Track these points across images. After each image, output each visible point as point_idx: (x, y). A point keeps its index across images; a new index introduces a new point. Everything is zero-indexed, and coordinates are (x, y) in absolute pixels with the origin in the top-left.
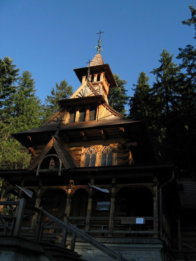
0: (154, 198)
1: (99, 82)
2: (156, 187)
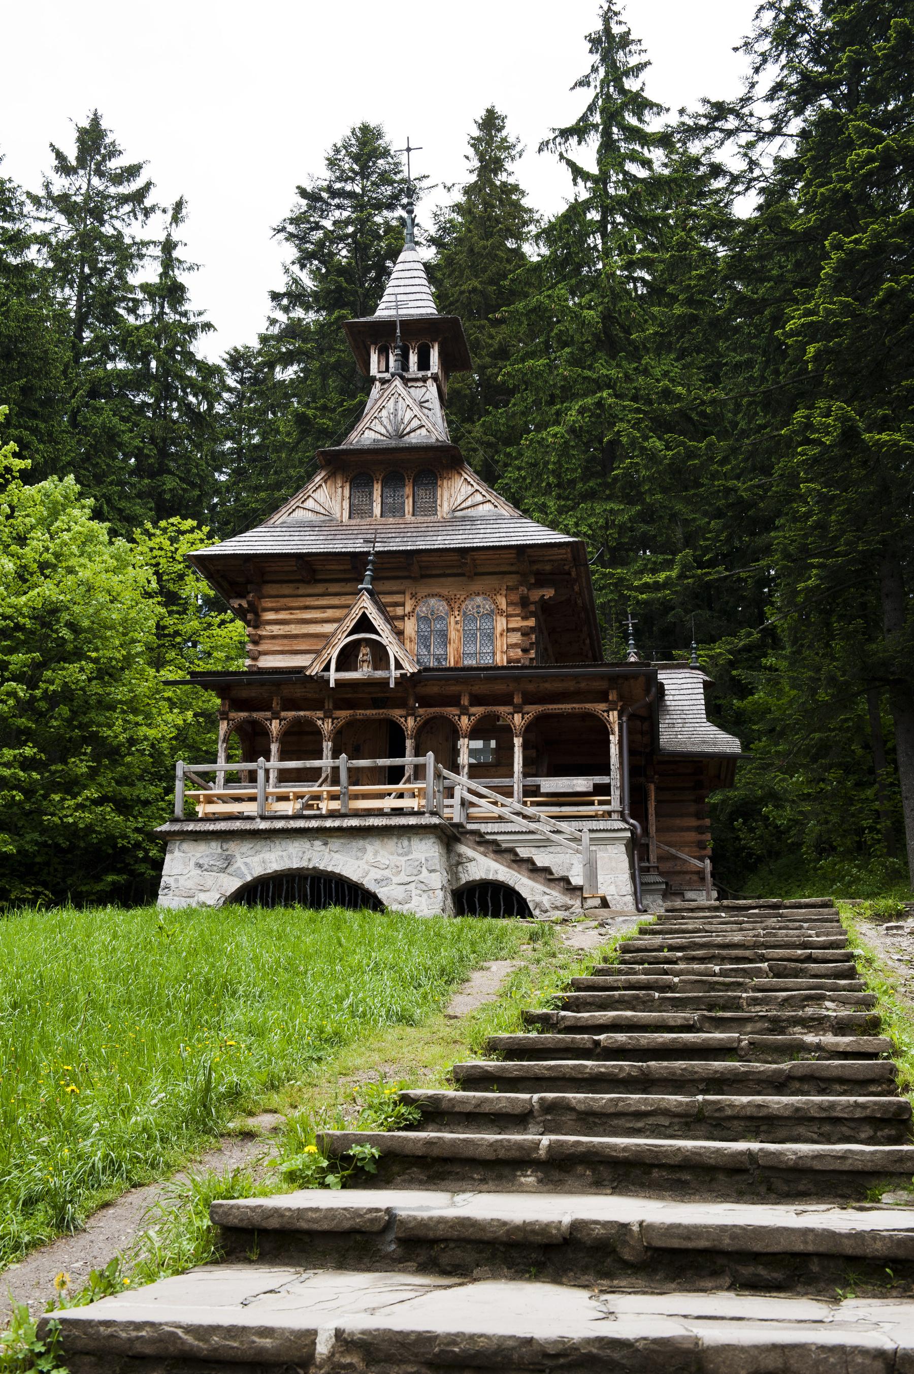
0: (611, 737)
1: (429, 374)
2: (616, 713)
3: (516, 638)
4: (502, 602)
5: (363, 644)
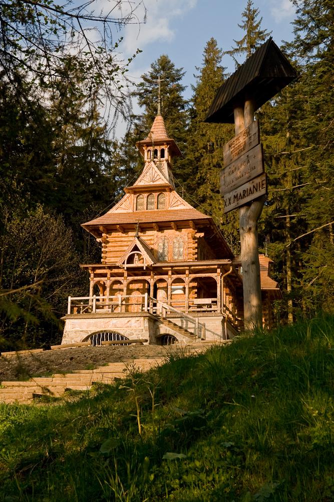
1: (164, 159)
5: (136, 255)
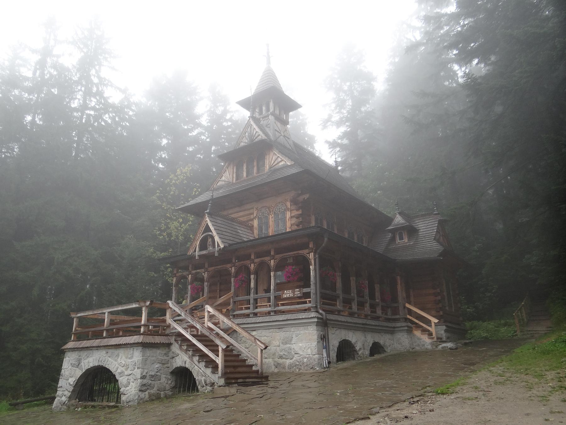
2: (312, 253)
3: (294, 221)
4: (288, 204)
